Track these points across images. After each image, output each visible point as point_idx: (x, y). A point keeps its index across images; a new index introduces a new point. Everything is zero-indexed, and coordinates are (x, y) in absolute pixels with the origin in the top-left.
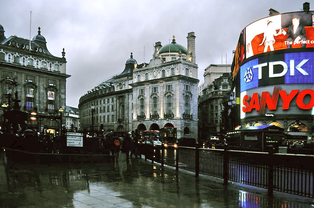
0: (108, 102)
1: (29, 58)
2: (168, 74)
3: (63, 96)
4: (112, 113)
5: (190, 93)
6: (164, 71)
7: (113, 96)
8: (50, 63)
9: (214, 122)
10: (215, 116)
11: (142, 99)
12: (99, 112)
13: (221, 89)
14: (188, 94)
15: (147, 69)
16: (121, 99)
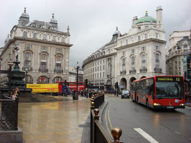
0: (101, 63)
1: (43, 34)
2: (143, 38)
3: (67, 60)
4: (104, 71)
5: (159, 52)
6: (139, 37)
7: (104, 59)
8: (58, 37)
9: (178, 73)
10: (178, 69)
11: (124, 59)
12: (95, 71)
13: (183, 48)
14: (158, 53)
15: (127, 37)
16: (109, 60)
